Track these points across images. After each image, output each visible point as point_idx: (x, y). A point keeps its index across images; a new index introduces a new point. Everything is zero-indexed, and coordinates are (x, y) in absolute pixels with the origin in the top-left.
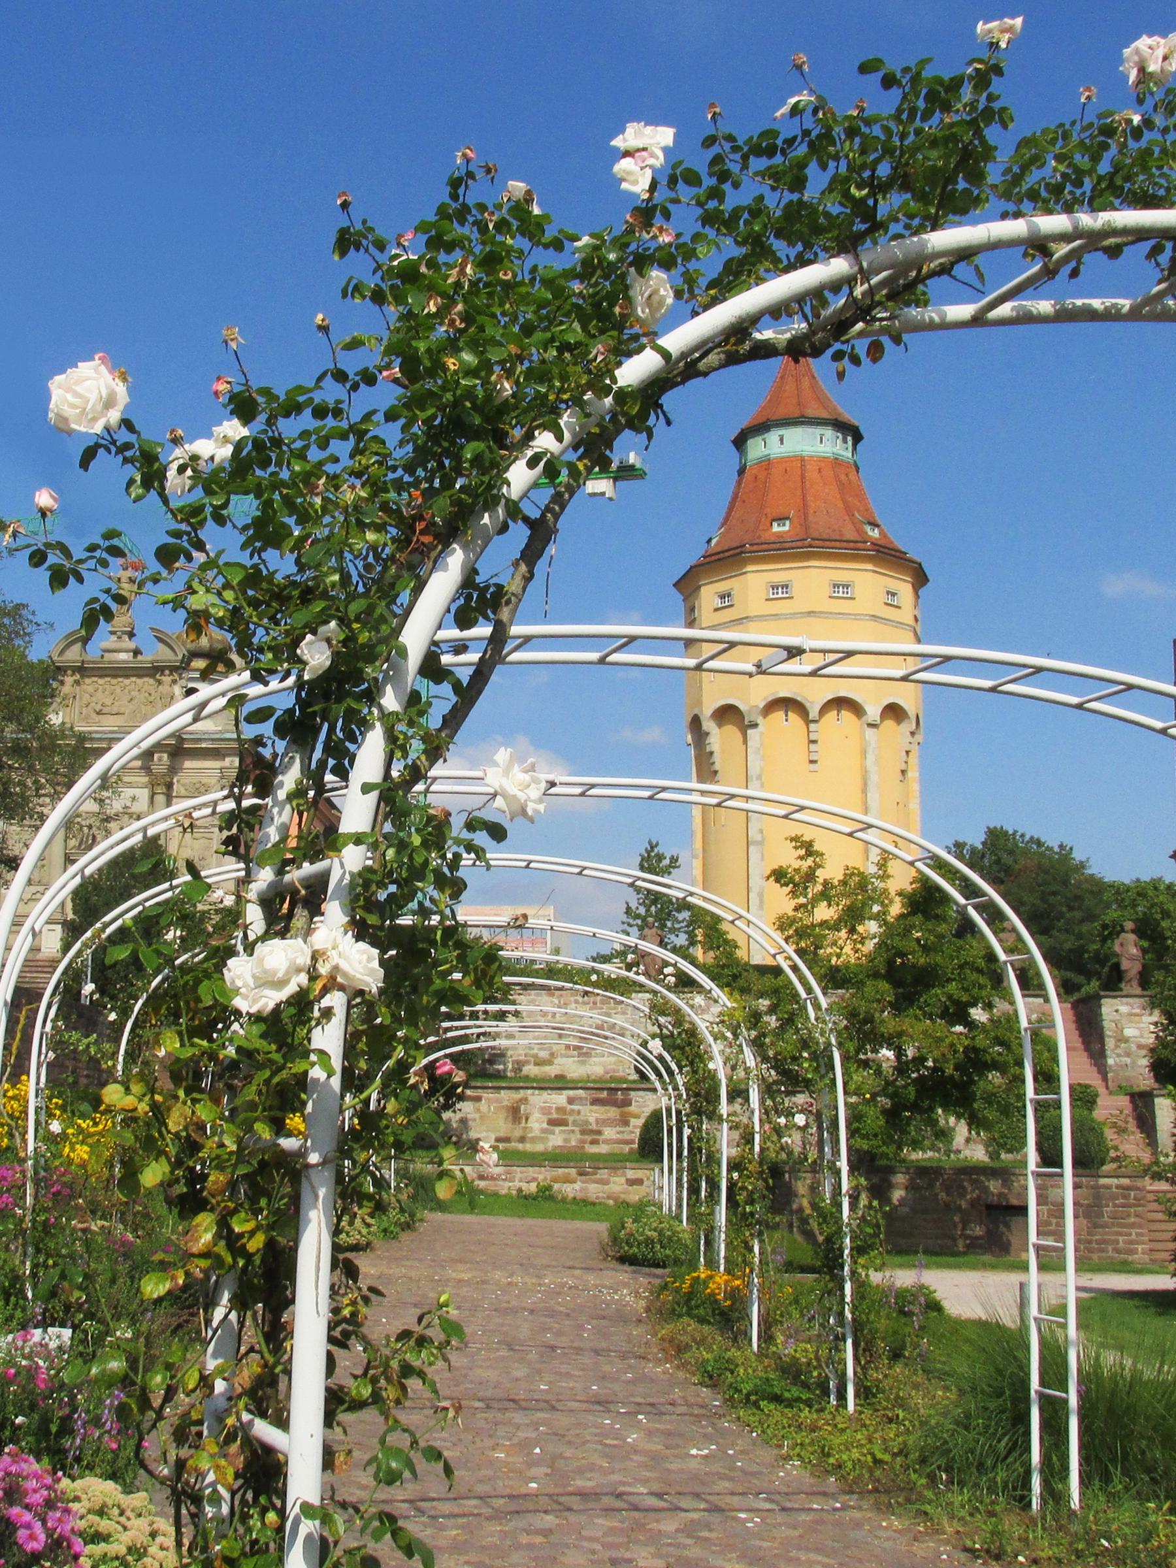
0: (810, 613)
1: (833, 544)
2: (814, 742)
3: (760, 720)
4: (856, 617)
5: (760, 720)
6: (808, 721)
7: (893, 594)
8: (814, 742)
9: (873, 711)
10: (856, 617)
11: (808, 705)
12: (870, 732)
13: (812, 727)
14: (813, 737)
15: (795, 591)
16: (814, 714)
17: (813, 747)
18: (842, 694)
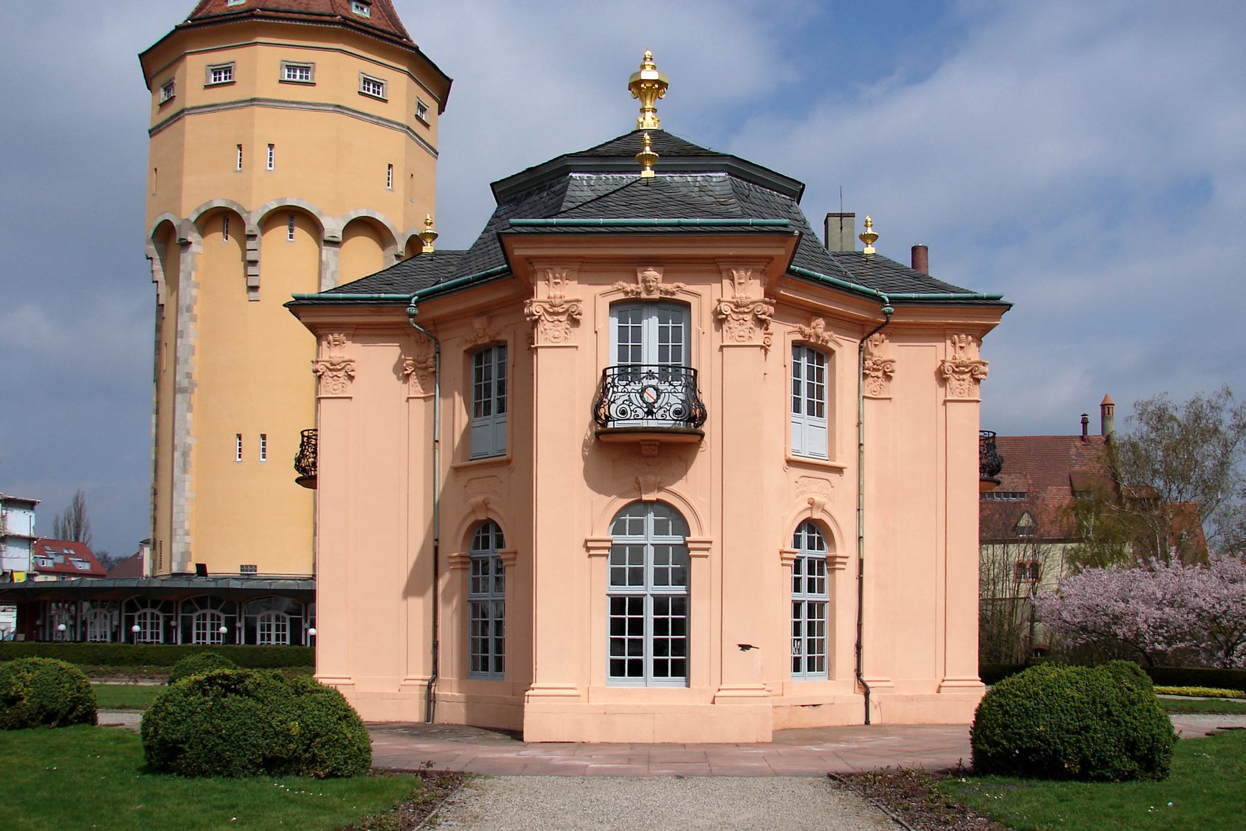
0: (253, 101)
1: (290, 15)
2: (254, 263)
3: (193, 237)
4: (316, 107)
5: (193, 237)
6: (245, 238)
7: (378, 85)
8: (254, 263)
9: (333, 226)
10: (316, 107)
11: (244, 216)
12: (328, 252)
13: (250, 244)
14: (251, 256)
15: (237, 75)
16: (252, 224)
17: (251, 270)
18: (291, 202)
